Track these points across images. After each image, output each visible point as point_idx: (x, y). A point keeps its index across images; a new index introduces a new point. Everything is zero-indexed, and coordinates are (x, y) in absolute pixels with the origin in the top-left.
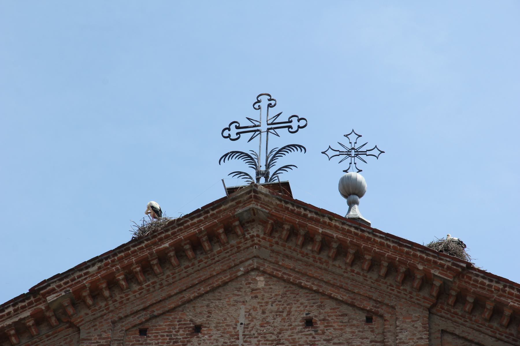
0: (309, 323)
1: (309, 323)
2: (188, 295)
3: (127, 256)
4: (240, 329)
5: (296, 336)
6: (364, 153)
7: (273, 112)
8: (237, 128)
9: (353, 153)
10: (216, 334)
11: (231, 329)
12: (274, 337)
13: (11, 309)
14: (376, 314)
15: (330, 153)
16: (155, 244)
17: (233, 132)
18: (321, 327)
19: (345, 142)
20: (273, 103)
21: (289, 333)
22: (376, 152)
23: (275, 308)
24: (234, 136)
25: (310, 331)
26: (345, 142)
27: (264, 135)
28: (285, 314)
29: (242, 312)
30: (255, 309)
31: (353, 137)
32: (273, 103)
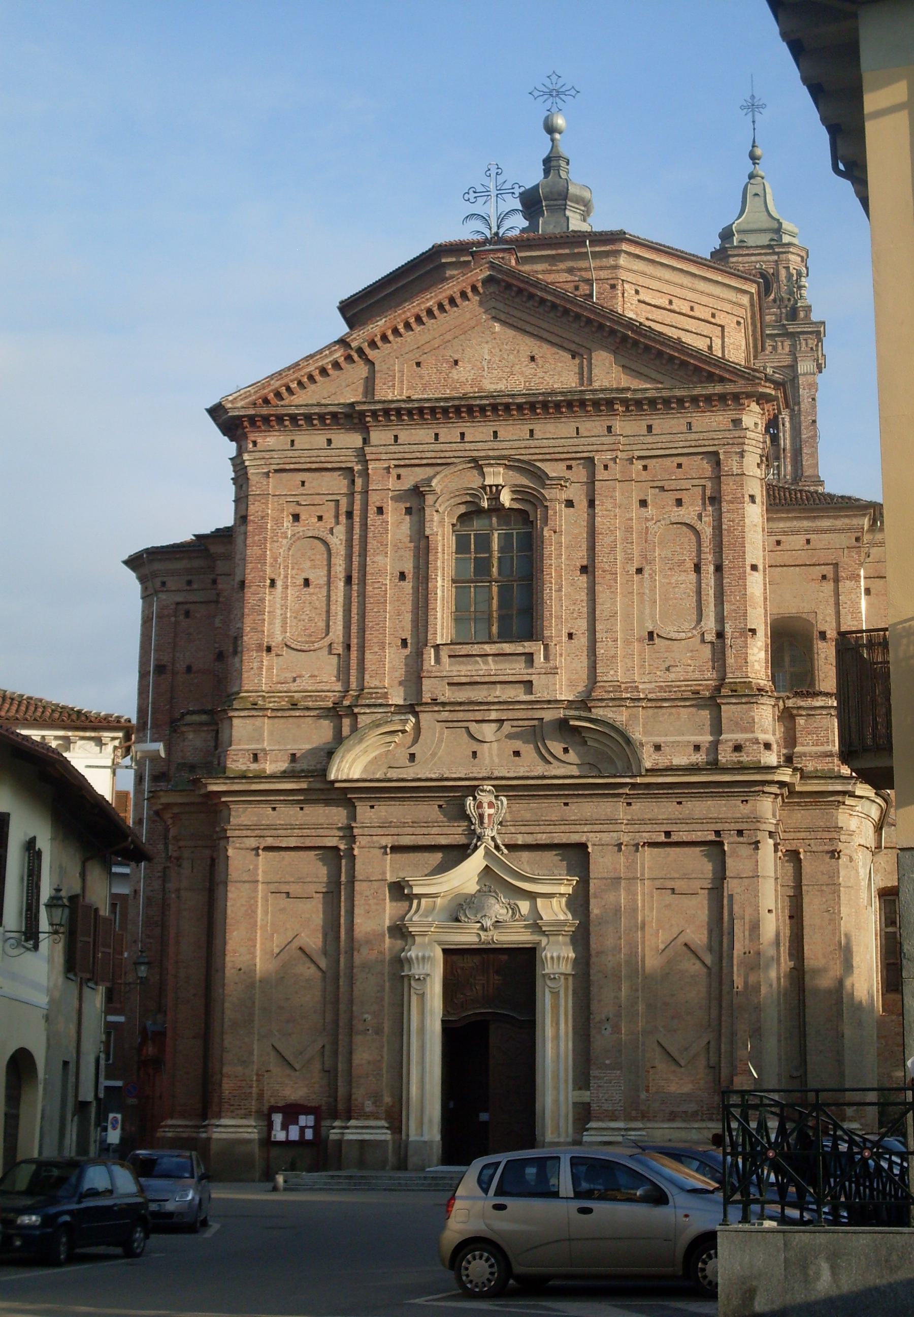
0: (533, 359)
1: (533, 359)
2: (448, 337)
3: (405, 312)
4: (485, 363)
5: (524, 369)
6: (564, 93)
7: (501, 179)
8: (475, 192)
9: (554, 93)
10: (469, 367)
11: (479, 363)
12: (508, 370)
13: (327, 352)
14: (578, 354)
15: (536, 93)
16: (423, 302)
17: (472, 195)
18: (540, 361)
19: (547, 82)
20: (500, 171)
21: (518, 367)
22: (573, 92)
23: (507, 347)
24: (472, 200)
25: (533, 365)
26: (547, 82)
27: (494, 199)
28: (515, 352)
29: (486, 351)
30: (494, 348)
31: (554, 78)
32: (500, 171)
